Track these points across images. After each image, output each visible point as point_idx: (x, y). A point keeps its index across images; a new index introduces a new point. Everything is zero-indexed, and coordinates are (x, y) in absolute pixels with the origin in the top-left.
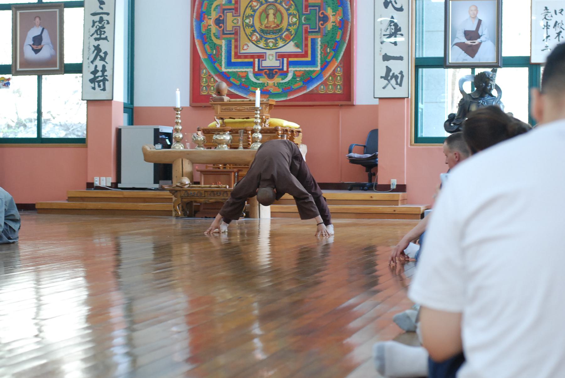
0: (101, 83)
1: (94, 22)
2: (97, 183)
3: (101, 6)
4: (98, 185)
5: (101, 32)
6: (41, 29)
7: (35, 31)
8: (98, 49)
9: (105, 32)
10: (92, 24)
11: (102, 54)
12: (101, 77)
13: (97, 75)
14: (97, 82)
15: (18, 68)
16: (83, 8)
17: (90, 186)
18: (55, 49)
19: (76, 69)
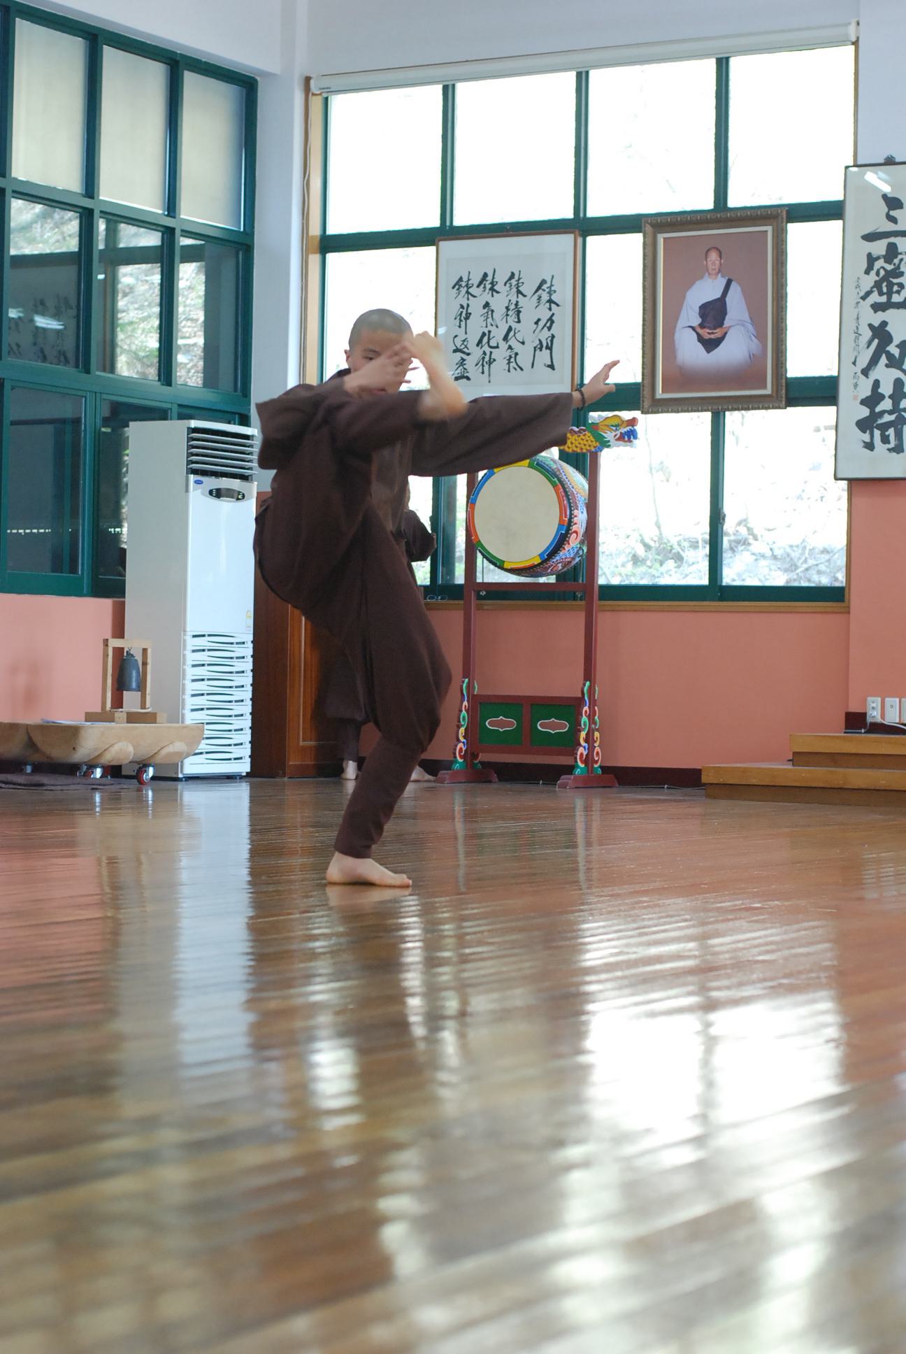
0: (891, 432)
1: (871, 260)
2: (874, 715)
3: (892, 213)
4: (879, 720)
5: (890, 285)
6: (721, 282)
7: (707, 290)
8: (881, 334)
9: (901, 286)
10: (865, 266)
11: (893, 349)
12: (890, 412)
13: (878, 409)
14: (879, 427)
15: (659, 393)
16: (840, 222)
17: (856, 721)
18: (761, 336)
19: (820, 392)
